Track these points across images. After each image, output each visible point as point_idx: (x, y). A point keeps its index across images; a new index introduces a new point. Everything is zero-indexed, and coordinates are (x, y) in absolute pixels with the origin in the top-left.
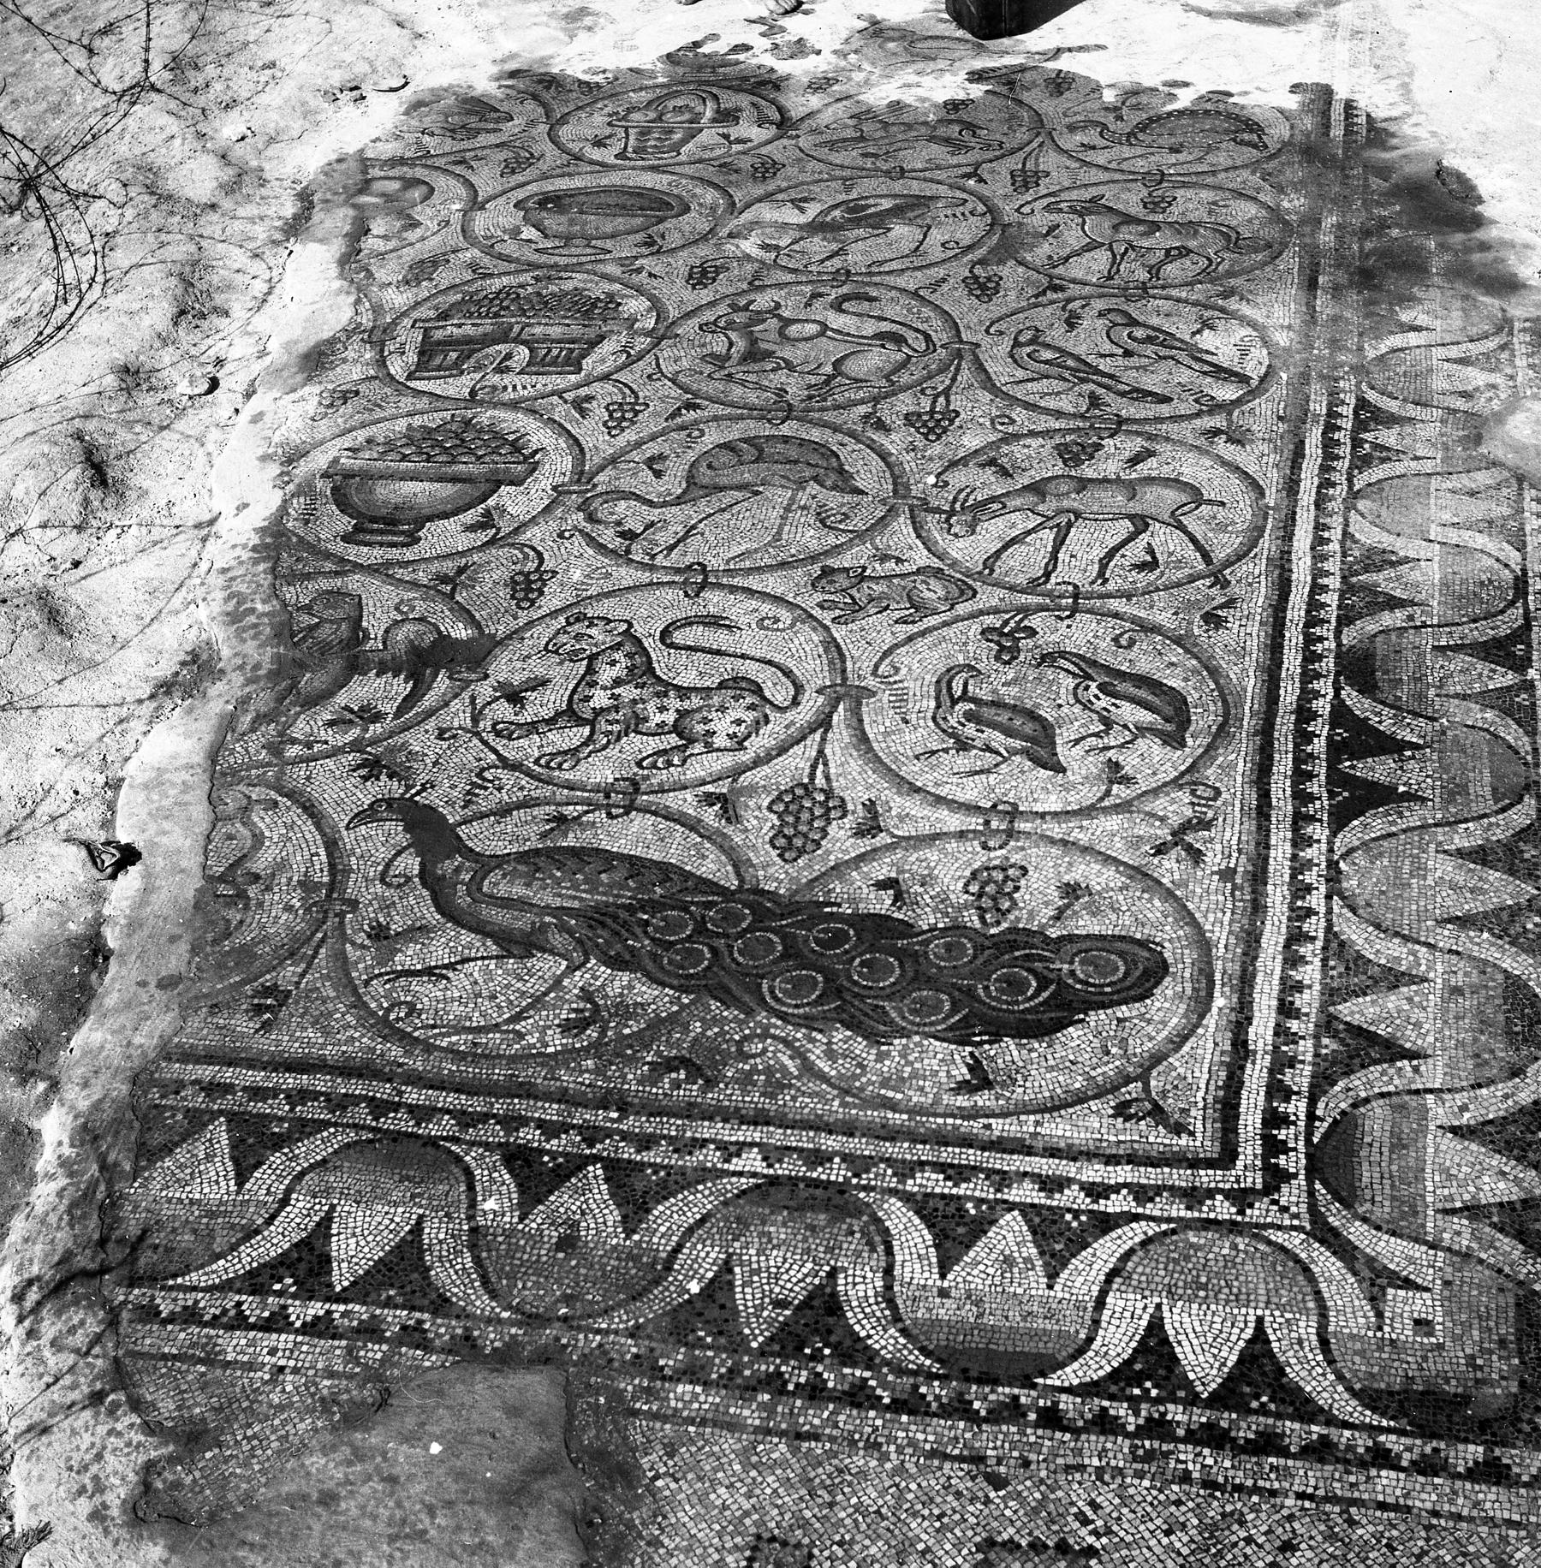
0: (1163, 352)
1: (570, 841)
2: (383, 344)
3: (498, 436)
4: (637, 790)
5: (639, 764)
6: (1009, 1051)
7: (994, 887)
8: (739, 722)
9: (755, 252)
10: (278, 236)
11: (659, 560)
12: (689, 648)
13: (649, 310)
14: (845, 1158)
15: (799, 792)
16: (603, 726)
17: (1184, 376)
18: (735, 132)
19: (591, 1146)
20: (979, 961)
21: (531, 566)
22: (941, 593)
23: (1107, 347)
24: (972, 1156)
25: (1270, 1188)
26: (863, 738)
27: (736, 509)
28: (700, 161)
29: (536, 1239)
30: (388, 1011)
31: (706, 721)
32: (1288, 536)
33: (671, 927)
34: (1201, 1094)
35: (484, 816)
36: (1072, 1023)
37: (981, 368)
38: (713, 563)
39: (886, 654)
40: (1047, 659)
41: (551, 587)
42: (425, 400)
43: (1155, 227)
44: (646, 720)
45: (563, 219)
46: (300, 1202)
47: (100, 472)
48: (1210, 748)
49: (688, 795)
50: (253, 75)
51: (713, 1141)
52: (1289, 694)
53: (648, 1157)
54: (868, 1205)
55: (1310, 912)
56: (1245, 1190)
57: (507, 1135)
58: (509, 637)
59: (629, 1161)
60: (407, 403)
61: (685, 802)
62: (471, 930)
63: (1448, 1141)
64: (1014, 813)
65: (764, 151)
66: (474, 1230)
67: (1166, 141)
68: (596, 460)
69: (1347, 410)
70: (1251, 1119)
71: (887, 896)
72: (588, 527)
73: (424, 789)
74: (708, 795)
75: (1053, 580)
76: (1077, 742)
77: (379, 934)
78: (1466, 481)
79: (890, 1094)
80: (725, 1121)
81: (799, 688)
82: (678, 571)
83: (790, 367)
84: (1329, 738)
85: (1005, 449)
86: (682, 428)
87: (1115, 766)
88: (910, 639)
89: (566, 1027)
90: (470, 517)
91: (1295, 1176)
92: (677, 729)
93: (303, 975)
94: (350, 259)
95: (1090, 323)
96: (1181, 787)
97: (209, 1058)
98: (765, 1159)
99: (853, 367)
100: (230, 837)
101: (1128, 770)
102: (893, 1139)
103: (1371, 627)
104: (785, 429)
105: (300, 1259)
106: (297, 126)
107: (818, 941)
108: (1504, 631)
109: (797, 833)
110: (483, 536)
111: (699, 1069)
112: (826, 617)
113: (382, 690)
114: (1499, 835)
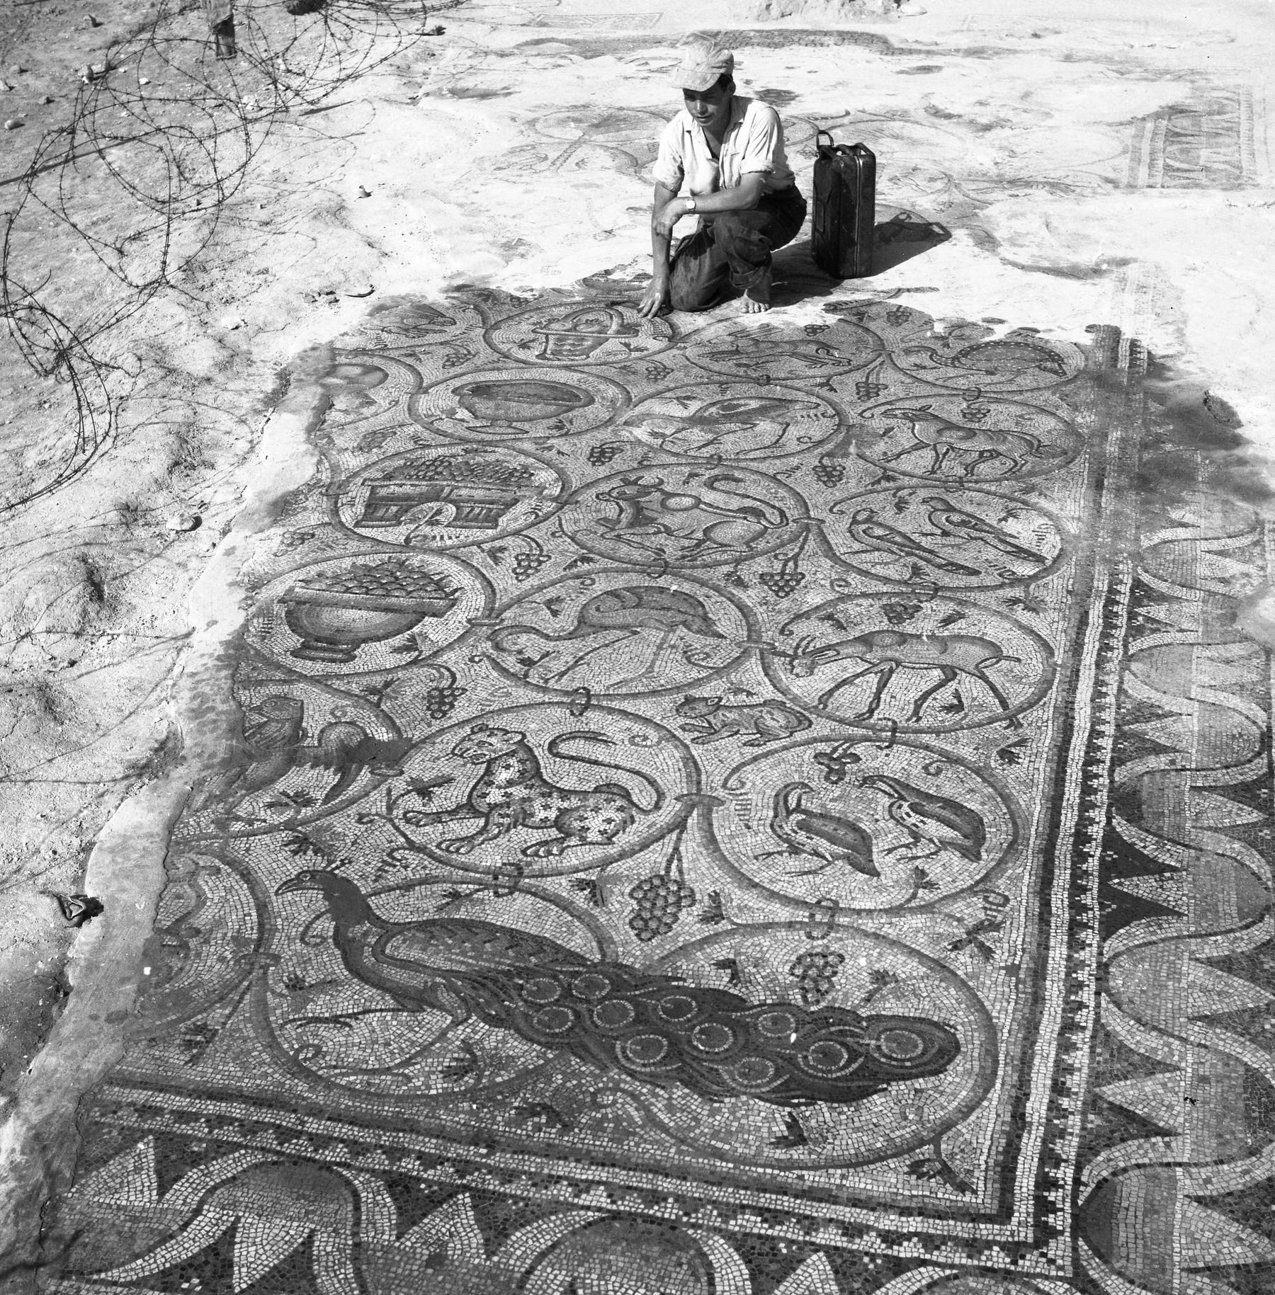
0: (975, 534)
1: (462, 914)
2: (337, 497)
3: (425, 576)
4: (521, 874)
5: (524, 852)
6: (820, 1114)
7: (817, 971)
8: (609, 821)
9: (645, 438)
10: (259, 406)
11: (551, 683)
12: (572, 758)
13: (556, 481)
14: (679, 1199)
15: (656, 882)
16: (495, 818)
17: (990, 554)
18: (634, 342)
19: (462, 1177)
21: (445, 683)
22: (783, 722)
23: (928, 528)
24: (786, 1203)
25: (1039, 1243)
27: (617, 645)
28: (605, 364)
29: (409, 1256)
30: (298, 1051)
31: (582, 819)
32: (1072, 689)
33: (542, 991)
34: (983, 1158)
35: (391, 889)
36: (876, 1092)
37: (825, 540)
38: (596, 688)
39: (735, 770)
40: (868, 781)
42: (369, 544)
43: (971, 434)
45: (491, 404)
46: (210, 1213)
47: (97, 588)
48: (1001, 862)
49: (564, 881)
50: (250, 279)
51: (566, 1178)
52: (1069, 820)
53: (509, 1189)
54: (695, 1240)
55: (1081, 1005)
56: (1018, 1244)
57: (392, 1164)
58: (423, 741)
60: (353, 545)
61: (560, 885)
62: (373, 985)
63: (1194, 1210)
64: (835, 909)
65: (657, 358)
66: (357, 1245)
67: (983, 365)
68: (505, 600)
69: (1125, 589)
70: (1025, 1182)
71: (726, 975)
72: (494, 654)
73: (343, 864)
74: (581, 881)
75: (876, 716)
76: (890, 851)
77: (296, 985)
78: (1222, 651)
79: (719, 1145)
80: (578, 1161)
81: (661, 795)
82: (567, 693)
83: (669, 531)
84: (1102, 859)
85: (841, 606)
86: (577, 577)
87: (921, 873)
88: (755, 759)
89: (448, 1073)
90: (398, 640)
91: (1062, 1233)
92: (557, 824)
93: (229, 1017)
94: (317, 427)
95: (916, 508)
96: (976, 893)
97: (144, 1085)
98: (609, 1196)
99: (720, 535)
100: (179, 897)
102: (719, 1184)
103: (1140, 768)
104: (661, 582)
105: (206, 1263)
106: (281, 320)
107: (665, 1011)
108: (1251, 777)
110: (408, 657)
111: (558, 1114)
112: (687, 737)
113: (314, 780)
114: (1242, 947)
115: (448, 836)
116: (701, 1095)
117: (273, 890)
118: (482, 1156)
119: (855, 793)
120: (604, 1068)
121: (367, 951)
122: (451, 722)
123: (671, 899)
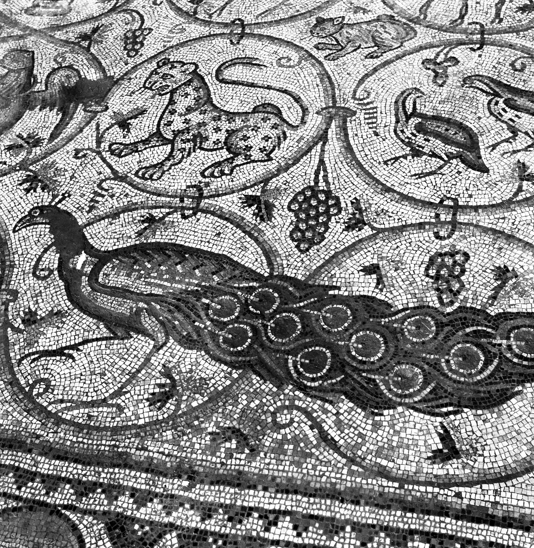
4: (201, 195)
5: (202, 174)
6: (468, 423)
8: (266, 138)
11: (215, 18)
12: (234, 83)
16: (179, 145)
19: (169, 514)
20: (441, 337)
21: (136, 26)
26: (349, 148)
30: (32, 387)
31: (245, 138)
38: (249, 19)
39: (362, 81)
40: (468, 81)
41: (149, 40)
49: (235, 197)
51: (256, 509)
57: (110, 504)
58: (122, 78)
59: (196, 530)
61: (231, 203)
62: (90, 315)
64: (456, 208)
73: (64, 198)
74: (248, 197)
76: (494, 147)
77: (30, 319)
79: (384, 463)
80: (265, 489)
81: (305, 110)
82: (226, 25)
87: (522, 167)
88: (375, 70)
98: (295, 528)
109: (310, 228)
112: (320, 55)
115: (145, 164)
116: (364, 409)
117: (11, 228)
118: (185, 489)
119: (458, 93)
120: (280, 387)
121: (84, 279)
122: (142, 59)
123: (321, 209)
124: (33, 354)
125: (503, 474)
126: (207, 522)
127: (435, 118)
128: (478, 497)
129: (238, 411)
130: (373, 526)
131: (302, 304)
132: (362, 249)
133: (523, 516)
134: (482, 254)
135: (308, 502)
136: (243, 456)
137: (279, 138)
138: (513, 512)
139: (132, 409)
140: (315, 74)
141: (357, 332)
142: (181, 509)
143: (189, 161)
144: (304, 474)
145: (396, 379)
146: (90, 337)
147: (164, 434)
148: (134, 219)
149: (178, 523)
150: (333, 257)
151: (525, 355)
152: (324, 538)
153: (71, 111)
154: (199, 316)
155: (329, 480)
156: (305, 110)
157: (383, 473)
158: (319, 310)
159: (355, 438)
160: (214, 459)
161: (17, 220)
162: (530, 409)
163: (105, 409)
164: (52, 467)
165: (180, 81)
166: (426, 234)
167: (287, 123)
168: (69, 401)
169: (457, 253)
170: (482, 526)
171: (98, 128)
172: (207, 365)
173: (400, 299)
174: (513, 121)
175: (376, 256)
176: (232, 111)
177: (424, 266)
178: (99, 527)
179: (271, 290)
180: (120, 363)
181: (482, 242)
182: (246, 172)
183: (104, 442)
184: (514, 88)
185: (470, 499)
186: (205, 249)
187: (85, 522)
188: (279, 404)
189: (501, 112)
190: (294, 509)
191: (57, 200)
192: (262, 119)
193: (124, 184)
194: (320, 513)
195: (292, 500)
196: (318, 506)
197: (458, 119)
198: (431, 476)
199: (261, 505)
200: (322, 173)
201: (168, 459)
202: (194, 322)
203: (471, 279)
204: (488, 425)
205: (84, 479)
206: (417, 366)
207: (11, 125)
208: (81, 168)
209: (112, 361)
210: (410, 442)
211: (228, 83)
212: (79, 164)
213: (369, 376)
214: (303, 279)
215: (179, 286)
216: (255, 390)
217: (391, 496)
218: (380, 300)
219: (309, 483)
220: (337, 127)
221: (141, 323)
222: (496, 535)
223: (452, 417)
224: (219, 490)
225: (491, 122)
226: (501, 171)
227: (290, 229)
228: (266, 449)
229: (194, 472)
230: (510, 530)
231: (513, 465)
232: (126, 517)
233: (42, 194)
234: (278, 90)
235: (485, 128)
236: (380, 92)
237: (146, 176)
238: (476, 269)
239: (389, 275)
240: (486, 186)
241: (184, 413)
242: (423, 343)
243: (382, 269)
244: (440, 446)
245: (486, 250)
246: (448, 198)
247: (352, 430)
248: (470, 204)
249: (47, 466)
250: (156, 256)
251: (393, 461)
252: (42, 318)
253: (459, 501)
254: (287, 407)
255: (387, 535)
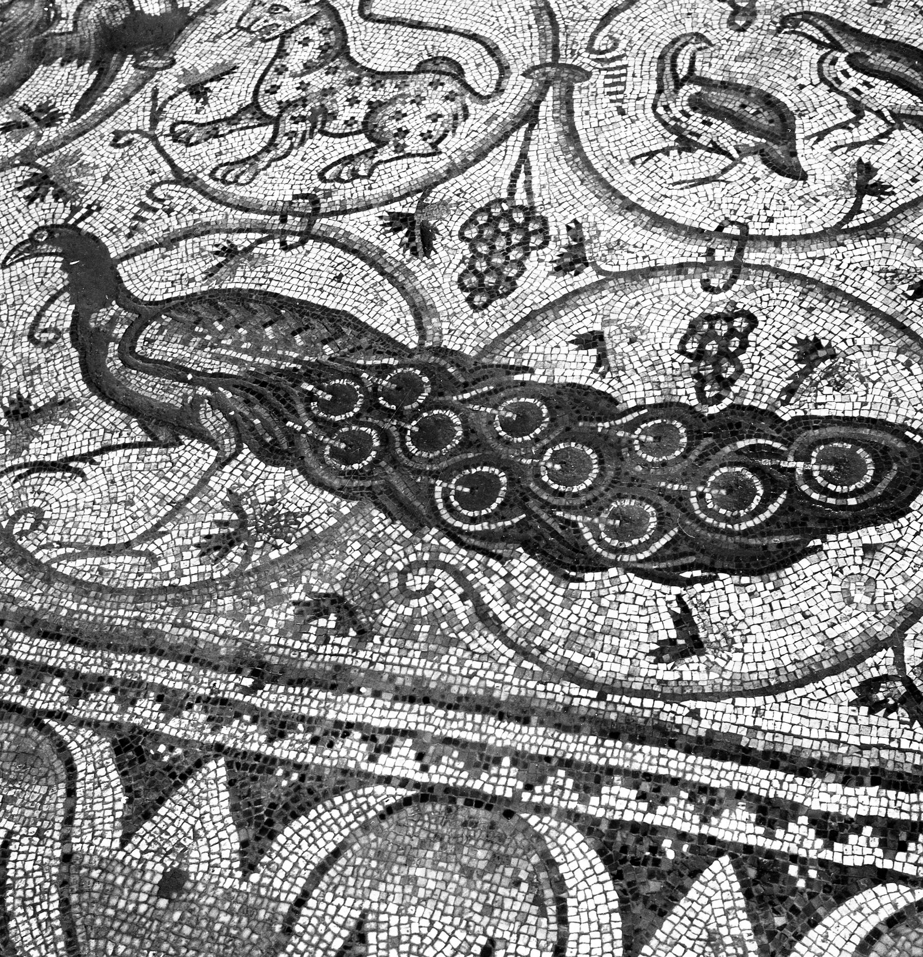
4: (316, 212)
5: (321, 176)
6: (724, 599)
7: (716, 345)
8: (435, 117)
16: (288, 125)
19: (215, 729)
26: (572, 135)
29: (135, 875)
30: (13, 520)
33: (341, 400)
35: (149, 247)
39: (605, 20)
44: (334, 116)
49: (372, 216)
51: (359, 726)
53: (282, 750)
54: (539, 837)
57: (123, 710)
58: (202, 12)
59: (258, 756)
61: (365, 226)
62: (118, 406)
64: (744, 240)
66: (67, 858)
73: (90, 213)
74: (394, 216)
76: (821, 136)
79: (577, 658)
80: (377, 694)
81: (504, 70)
87: (866, 169)
92: (368, 129)
98: (419, 757)
101: (882, 176)
107: (506, 424)
109: (492, 269)
115: (225, 159)
116: (552, 570)
118: (247, 691)
119: (770, 43)
121: (113, 347)
123: (516, 238)
124: (19, 467)
125: (773, 682)
126: (276, 744)
127: (724, 85)
128: (726, 718)
129: (345, 567)
130: (548, 759)
131: (467, 396)
132: (578, 306)
133: (798, 750)
134: (779, 318)
135: (445, 718)
136: (346, 641)
137: (456, 117)
138: (782, 744)
139: (171, 559)
140: (528, 8)
141: (554, 443)
142: (236, 723)
143: (301, 154)
144: (443, 673)
145: (611, 522)
146: (114, 442)
147: (220, 602)
148: (202, 250)
149: (230, 744)
150: (528, 318)
151: (832, 487)
152: (465, 774)
153: (113, 69)
154: (295, 412)
155: (482, 684)
156: (504, 70)
157: (574, 675)
158: (495, 407)
159: (533, 618)
160: (298, 645)
161: (10, 248)
162: (829, 577)
163: (128, 559)
164: (34, 650)
165: (299, 17)
166: (687, 283)
167: (472, 90)
168: (70, 545)
169: (737, 315)
170: (727, 765)
171: (154, 97)
172: (300, 491)
173: (633, 392)
174: (859, 92)
175: (599, 318)
176: (380, 69)
177: (679, 336)
178: (102, 747)
179: (418, 372)
180: (159, 485)
181: (781, 297)
182: (394, 173)
183: (121, 612)
184: (867, 35)
185: (713, 721)
186: (315, 301)
187: (80, 739)
188: (413, 558)
189: (840, 76)
190: (421, 727)
191: (78, 216)
192: (431, 84)
193: (190, 190)
194: (463, 735)
195: (418, 713)
196: (461, 724)
197: (764, 88)
198: (653, 681)
199: (367, 720)
200: (522, 176)
201: (222, 643)
202: (286, 421)
203: (755, 360)
204: (757, 601)
205: (85, 670)
206: (649, 502)
207: (11, 89)
208: (121, 163)
209: (145, 481)
210: (624, 626)
211: (379, 21)
212: (118, 156)
213: (567, 516)
214: (474, 354)
215: (267, 362)
216: (375, 535)
217: (583, 712)
218: (599, 392)
219: (449, 686)
220: (555, 99)
221: (198, 421)
222: (750, 780)
223: (698, 587)
224: (301, 694)
225: (820, 93)
226: (828, 178)
227: (460, 270)
228: (384, 631)
229: (263, 664)
230: (773, 772)
231: (791, 668)
232: (147, 733)
233: (54, 205)
234: (462, 35)
235: (809, 105)
236: (635, 39)
237: (229, 178)
238: (766, 344)
239: (618, 350)
240: (799, 202)
241: (256, 570)
242: (664, 464)
243: (607, 340)
244: (673, 634)
245: (785, 312)
246: (732, 223)
247: (530, 603)
248: (768, 233)
249: (25, 648)
250: (233, 312)
251: (593, 656)
252: (38, 410)
253: (695, 724)
254: (426, 564)
255: (569, 775)
